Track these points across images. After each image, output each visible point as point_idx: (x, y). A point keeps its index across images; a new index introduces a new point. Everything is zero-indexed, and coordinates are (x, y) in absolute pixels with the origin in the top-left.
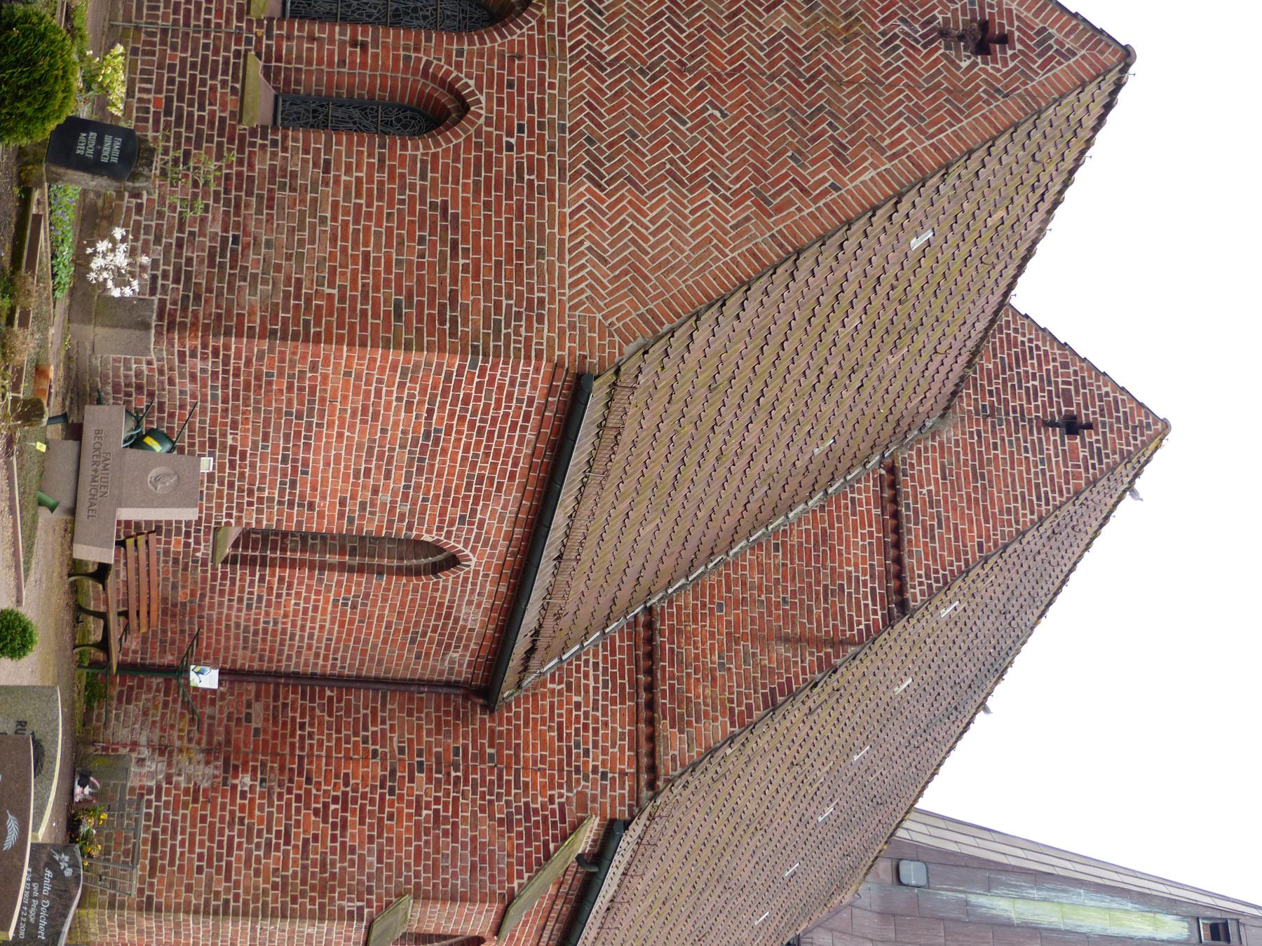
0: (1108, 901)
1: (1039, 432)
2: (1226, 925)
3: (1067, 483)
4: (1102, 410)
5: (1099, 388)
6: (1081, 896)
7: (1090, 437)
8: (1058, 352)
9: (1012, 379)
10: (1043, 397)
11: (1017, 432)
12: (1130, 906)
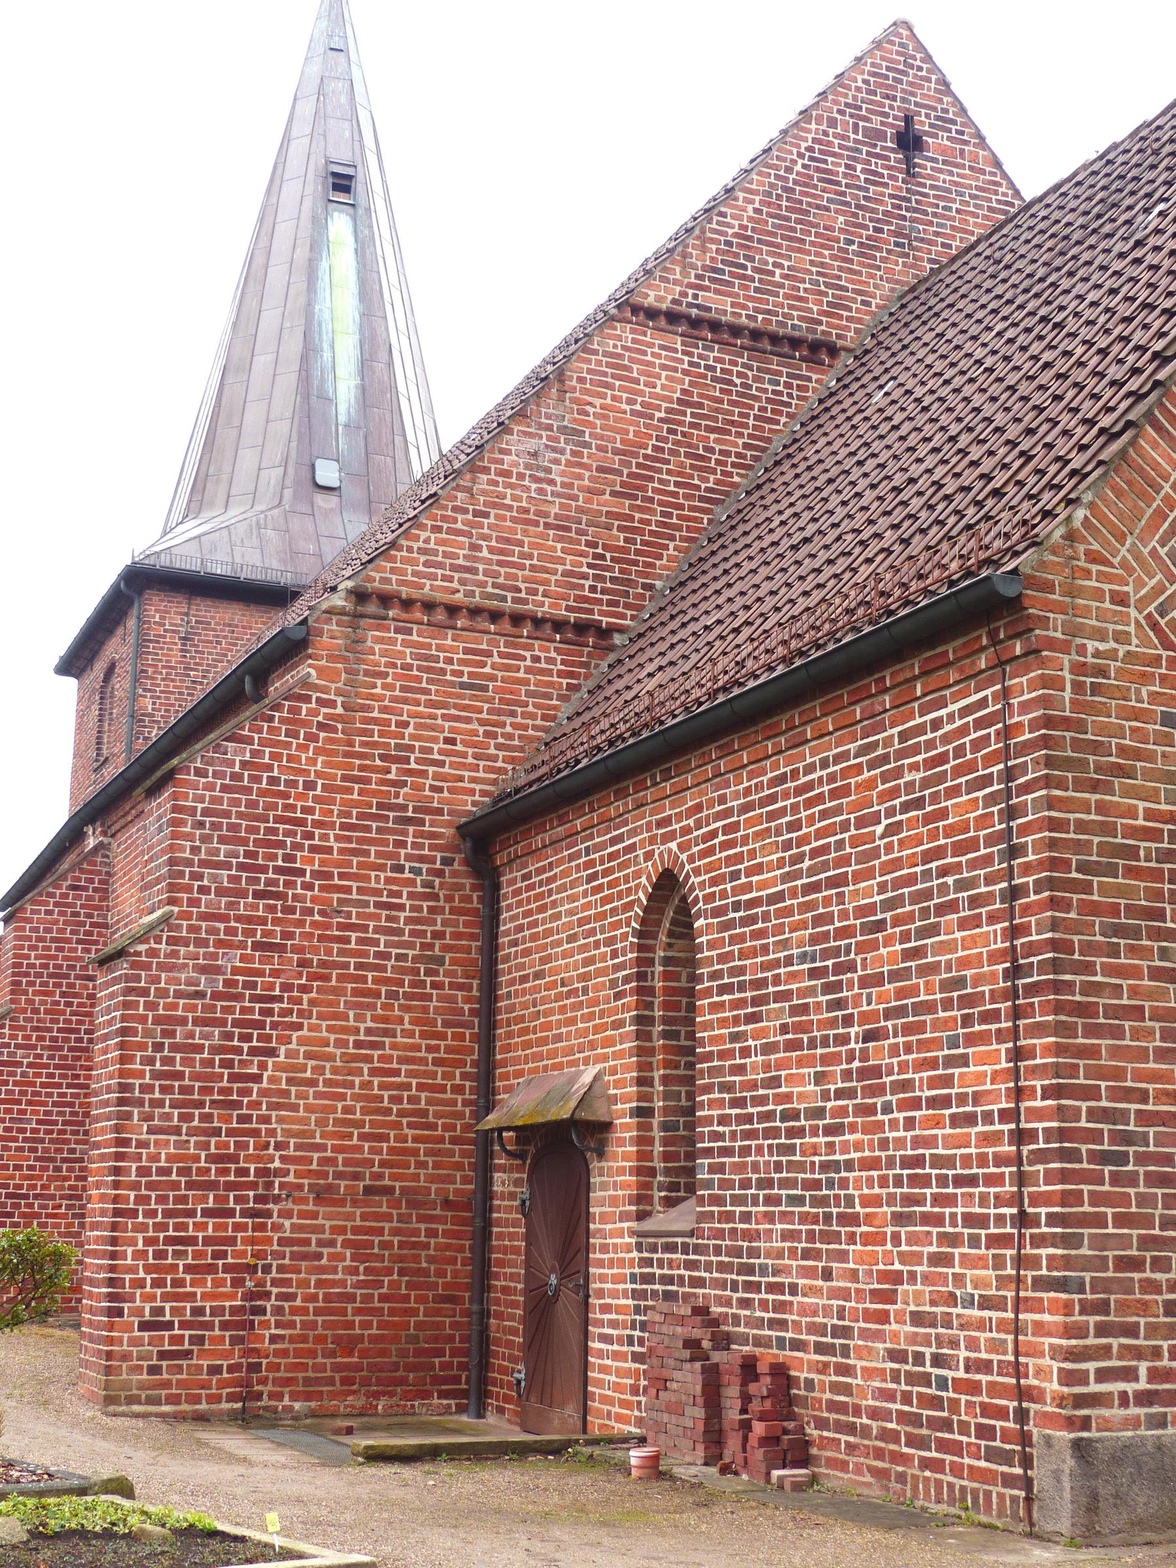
0: (323, 283)
1: (924, 185)
2: (334, 174)
3: (983, 172)
4: (887, 97)
5: (858, 89)
6: (322, 308)
7: (922, 123)
8: (813, 126)
9: (856, 197)
10: (876, 165)
11: (925, 213)
12: (324, 265)
